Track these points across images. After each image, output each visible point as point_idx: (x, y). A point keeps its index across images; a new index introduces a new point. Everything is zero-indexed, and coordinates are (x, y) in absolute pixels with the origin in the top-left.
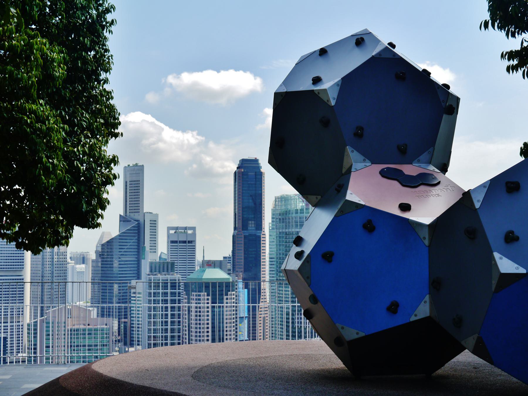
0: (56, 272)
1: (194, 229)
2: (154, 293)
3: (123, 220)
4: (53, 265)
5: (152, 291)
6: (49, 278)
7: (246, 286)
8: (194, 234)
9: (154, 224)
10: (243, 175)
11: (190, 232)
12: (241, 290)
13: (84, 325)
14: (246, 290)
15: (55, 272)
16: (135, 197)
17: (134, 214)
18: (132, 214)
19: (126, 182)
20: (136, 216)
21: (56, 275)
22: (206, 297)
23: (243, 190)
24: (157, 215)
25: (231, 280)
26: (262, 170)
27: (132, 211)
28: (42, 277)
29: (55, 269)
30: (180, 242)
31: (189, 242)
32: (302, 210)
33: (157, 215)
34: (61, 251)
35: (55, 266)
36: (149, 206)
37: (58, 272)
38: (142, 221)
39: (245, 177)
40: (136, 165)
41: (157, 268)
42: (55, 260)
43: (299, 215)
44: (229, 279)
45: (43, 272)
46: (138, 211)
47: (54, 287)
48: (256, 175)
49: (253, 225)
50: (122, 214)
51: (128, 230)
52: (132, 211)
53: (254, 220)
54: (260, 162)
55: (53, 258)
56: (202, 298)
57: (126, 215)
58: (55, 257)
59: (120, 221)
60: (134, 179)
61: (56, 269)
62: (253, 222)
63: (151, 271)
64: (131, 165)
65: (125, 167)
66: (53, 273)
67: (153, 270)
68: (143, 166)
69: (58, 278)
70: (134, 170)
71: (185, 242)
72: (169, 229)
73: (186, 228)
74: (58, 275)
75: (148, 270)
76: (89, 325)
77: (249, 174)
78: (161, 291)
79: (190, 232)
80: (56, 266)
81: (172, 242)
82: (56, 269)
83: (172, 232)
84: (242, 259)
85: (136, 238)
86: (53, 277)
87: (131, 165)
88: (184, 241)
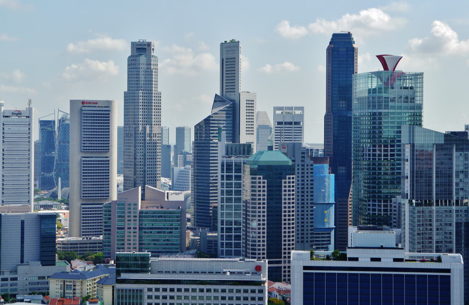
0: (149, 154)
1: (302, 109)
2: (227, 176)
3: (218, 100)
4: (145, 147)
5: (225, 174)
6: (141, 160)
7: (333, 170)
8: (302, 116)
9: (251, 104)
10: (333, 51)
11: (298, 112)
12: (327, 174)
13: (158, 207)
14: (333, 176)
15: (147, 154)
16: (231, 75)
17: (229, 93)
18: (228, 94)
19: (223, 60)
20: (232, 96)
21: (149, 157)
22: (262, 181)
23: (332, 67)
24: (255, 94)
25: (291, 163)
26: (354, 46)
27: (228, 90)
28: (135, 159)
29: (147, 151)
30: (286, 123)
31: (296, 123)
32: (380, 89)
33: (255, 94)
34: (153, 132)
35: (147, 148)
36: (246, 85)
37: (151, 154)
38: (237, 100)
39: (335, 53)
40: (232, 41)
41: (234, 150)
42: (147, 141)
43: (377, 94)
44: (288, 161)
45: (135, 154)
46: (234, 90)
47: (147, 170)
48: (347, 50)
49: (344, 106)
50: (219, 94)
51: (220, 110)
52: (228, 90)
53: (345, 100)
54: (353, 36)
55: (145, 140)
56: (257, 181)
57: (222, 95)
58: (147, 138)
59: (215, 101)
60: (230, 56)
61: (149, 151)
62: (344, 102)
63: (227, 154)
64: (228, 41)
65: (222, 43)
66: (145, 155)
67: (230, 152)
68: (238, 42)
69: (151, 160)
70: (230, 47)
71: (291, 123)
72: (276, 109)
73: (291, 108)
74: (151, 157)
75: (224, 152)
76: (162, 208)
77: (340, 49)
78: (234, 174)
79: (298, 112)
80: (149, 148)
81: (279, 123)
82: (149, 151)
83: (279, 112)
84: (331, 142)
85: (231, 119)
86: (145, 159)
87: (228, 41)
88: (290, 124)
